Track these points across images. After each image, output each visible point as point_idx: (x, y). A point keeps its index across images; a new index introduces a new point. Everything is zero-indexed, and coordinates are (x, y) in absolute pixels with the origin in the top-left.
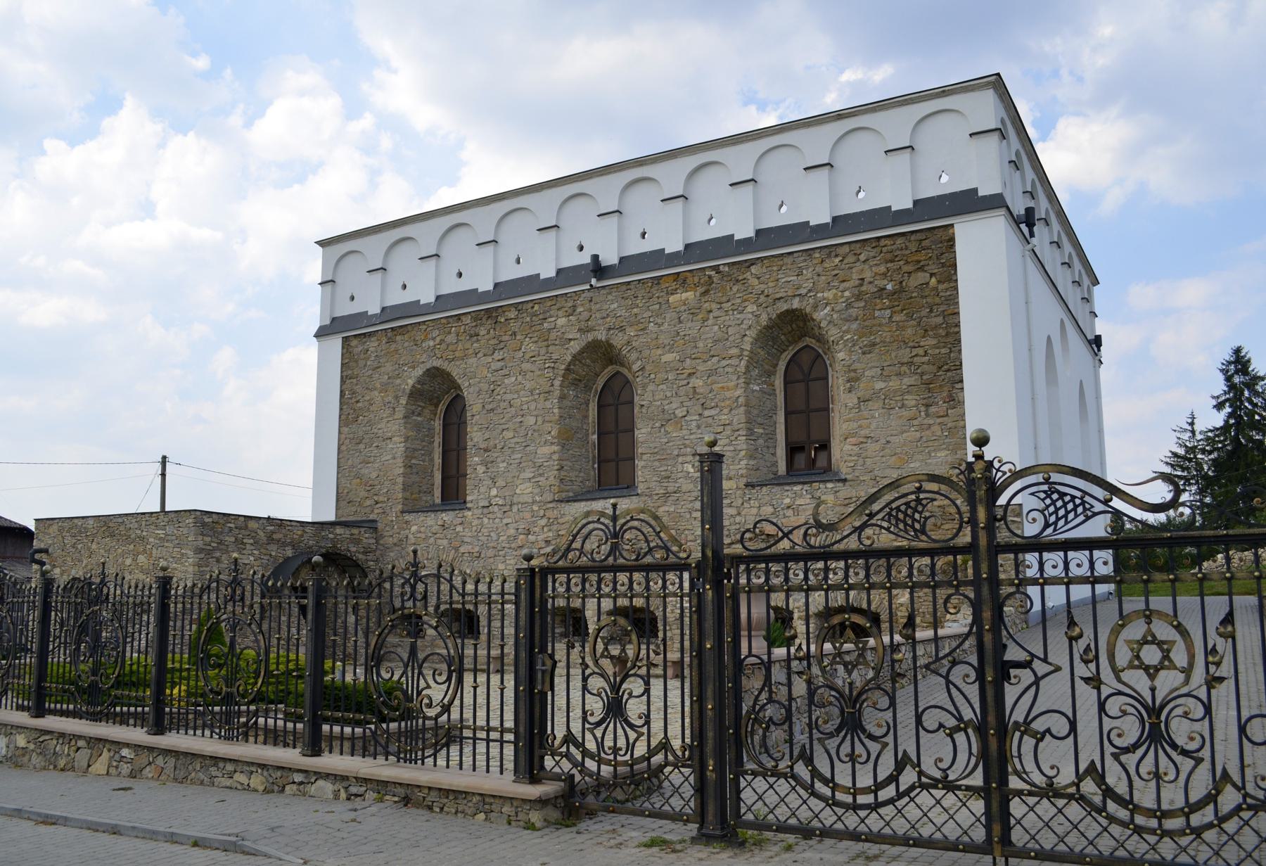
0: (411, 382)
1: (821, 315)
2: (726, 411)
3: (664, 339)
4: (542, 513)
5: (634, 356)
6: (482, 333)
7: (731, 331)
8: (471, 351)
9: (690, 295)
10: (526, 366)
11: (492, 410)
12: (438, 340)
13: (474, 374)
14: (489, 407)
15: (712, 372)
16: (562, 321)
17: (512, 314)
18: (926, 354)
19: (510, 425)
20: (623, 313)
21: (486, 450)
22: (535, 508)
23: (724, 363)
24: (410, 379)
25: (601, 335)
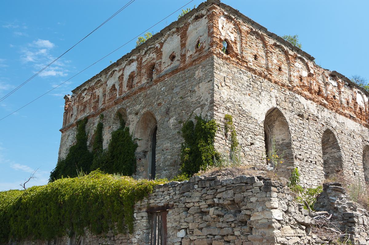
5: (339, 141)
6: (295, 103)
14: (300, 139)
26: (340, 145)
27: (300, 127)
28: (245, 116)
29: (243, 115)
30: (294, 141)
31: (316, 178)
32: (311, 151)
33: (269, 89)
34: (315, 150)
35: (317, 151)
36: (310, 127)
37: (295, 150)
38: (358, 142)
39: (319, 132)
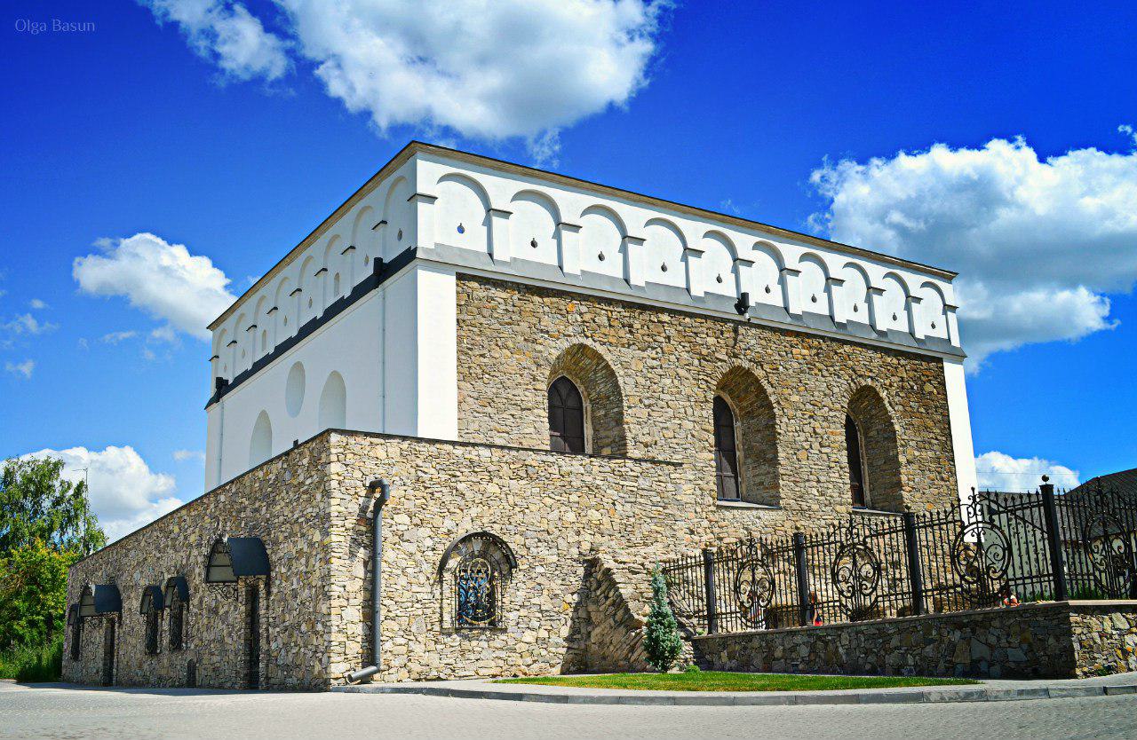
0: (556, 353)
1: (883, 394)
2: (835, 451)
3: (790, 382)
4: (704, 515)
5: (769, 390)
7: (836, 390)
8: (625, 341)
9: (805, 352)
10: (682, 372)
11: (649, 406)
12: (587, 317)
13: (630, 366)
14: (647, 402)
15: (826, 419)
16: (711, 340)
17: (665, 317)
18: (936, 439)
19: (668, 424)
20: (759, 350)
21: (646, 446)
22: (699, 510)
23: (832, 414)
24: (554, 349)
25: (746, 365)
26: (772, 399)
27: (649, 375)
28: (498, 374)
29: (492, 373)
30: (629, 407)
31: (692, 477)
32: (679, 422)
33: (563, 308)
34: (690, 419)
35: (697, 419)
36: (679, 371)
37: (632, 426)
38: (835, 384)
39: (705, 378)
